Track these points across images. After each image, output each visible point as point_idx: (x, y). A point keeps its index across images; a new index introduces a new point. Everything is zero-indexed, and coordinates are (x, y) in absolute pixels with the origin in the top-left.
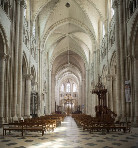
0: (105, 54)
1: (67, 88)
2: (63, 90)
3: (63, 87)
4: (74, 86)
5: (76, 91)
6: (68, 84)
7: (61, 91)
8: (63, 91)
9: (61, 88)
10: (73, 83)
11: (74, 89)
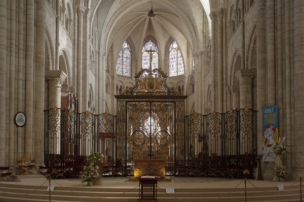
0: (251, 6)
1: (143, 61)
2: (129, 68)
3: (129, 56)
4: (173, 54)
5: (181, 73)
6: (150, 45)
7: (119, 72)
8: (128, 74)
9: (119, 61)
10: (171, 40)
11: (175, 64)
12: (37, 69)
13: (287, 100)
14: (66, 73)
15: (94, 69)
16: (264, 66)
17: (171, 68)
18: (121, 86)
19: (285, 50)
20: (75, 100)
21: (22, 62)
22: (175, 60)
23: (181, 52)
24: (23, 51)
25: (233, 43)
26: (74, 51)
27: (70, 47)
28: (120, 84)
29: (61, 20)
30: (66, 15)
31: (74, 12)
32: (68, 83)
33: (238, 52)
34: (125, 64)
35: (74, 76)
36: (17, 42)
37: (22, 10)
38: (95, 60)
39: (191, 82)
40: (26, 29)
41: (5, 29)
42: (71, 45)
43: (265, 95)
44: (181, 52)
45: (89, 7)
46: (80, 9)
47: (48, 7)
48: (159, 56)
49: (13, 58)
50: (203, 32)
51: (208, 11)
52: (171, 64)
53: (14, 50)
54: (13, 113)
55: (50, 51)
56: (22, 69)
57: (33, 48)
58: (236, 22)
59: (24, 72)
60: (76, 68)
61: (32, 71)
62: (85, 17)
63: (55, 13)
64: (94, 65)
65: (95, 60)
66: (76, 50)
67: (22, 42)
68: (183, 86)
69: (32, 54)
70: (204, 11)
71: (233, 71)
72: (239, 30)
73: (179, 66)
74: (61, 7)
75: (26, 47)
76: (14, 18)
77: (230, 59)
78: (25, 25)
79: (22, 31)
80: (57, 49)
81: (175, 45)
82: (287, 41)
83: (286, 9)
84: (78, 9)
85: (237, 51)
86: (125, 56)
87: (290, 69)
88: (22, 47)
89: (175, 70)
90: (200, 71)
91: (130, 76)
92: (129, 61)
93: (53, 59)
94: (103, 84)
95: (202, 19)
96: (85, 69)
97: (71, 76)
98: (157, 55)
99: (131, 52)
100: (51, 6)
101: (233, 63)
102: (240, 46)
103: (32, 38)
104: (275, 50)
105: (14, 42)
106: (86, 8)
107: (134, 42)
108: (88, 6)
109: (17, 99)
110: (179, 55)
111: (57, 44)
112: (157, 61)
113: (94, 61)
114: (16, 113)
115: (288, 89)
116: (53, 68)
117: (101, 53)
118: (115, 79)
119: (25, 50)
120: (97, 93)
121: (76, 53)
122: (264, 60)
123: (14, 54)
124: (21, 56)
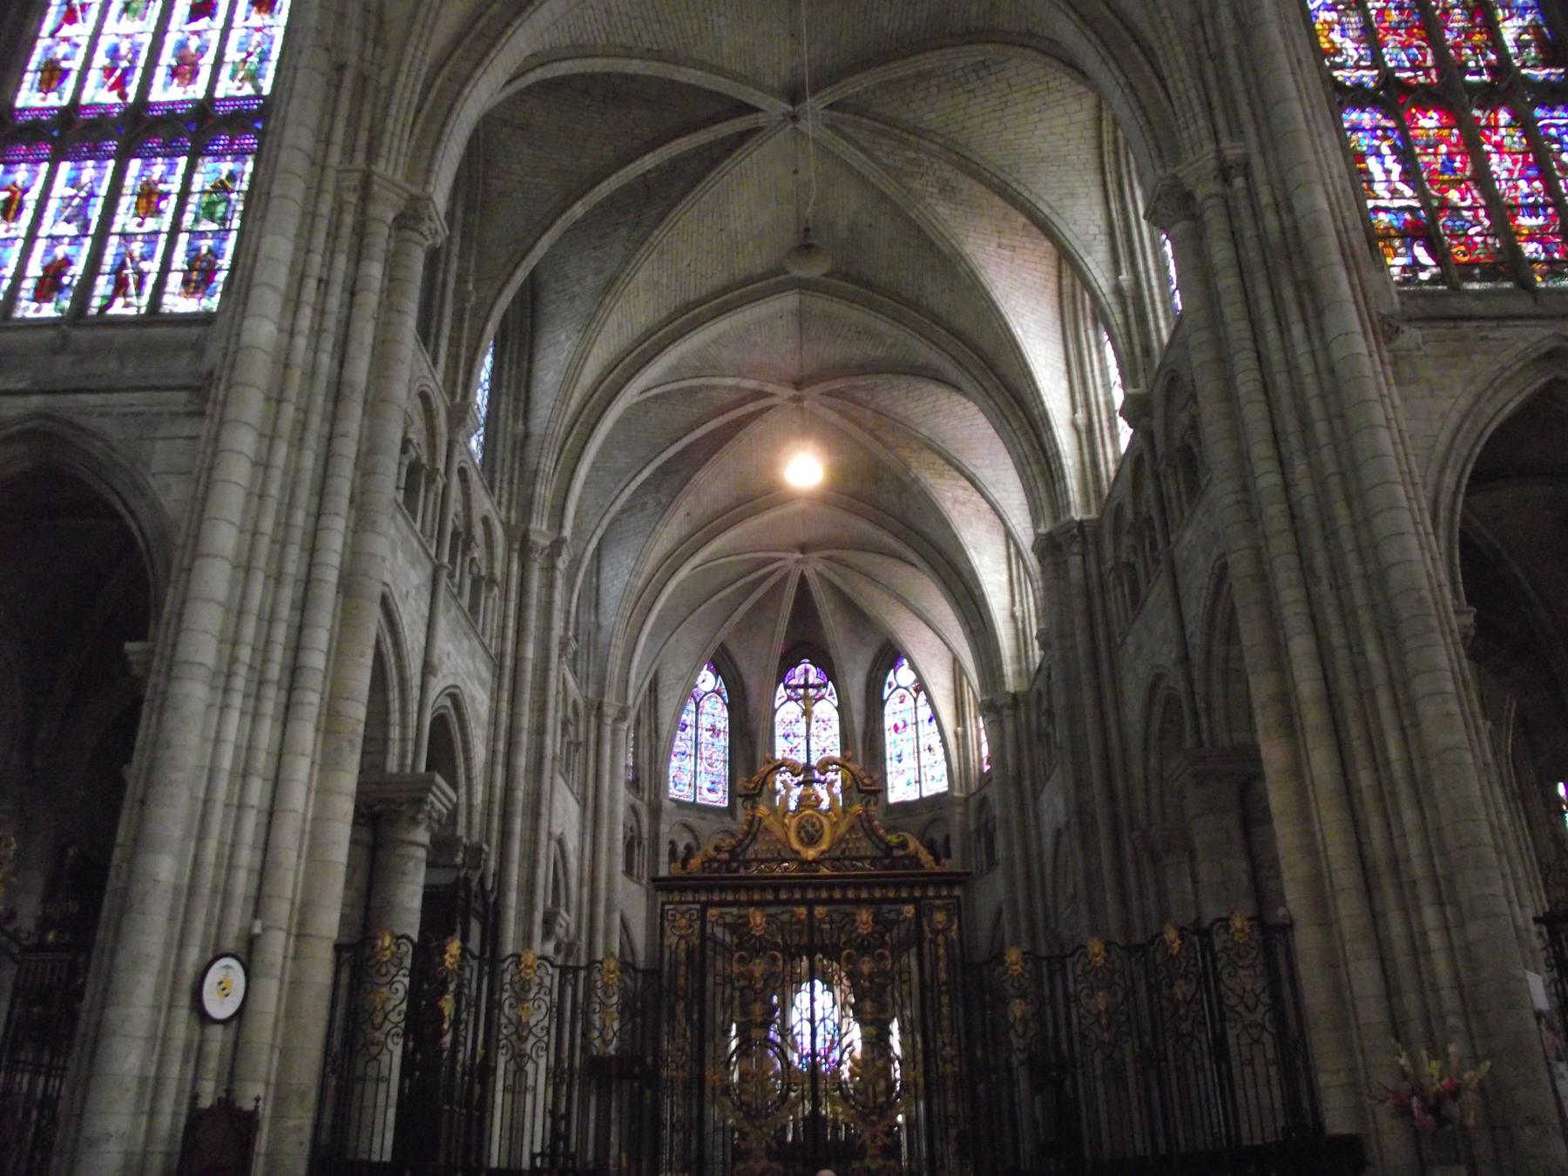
2: (722, 769)
3: (723, 724)
4: (896, 710)
8: (719, 799)
9: (682, 742)
11: (908, 749)
12: (328, 762)
13: (1418, 868)
14: (455, 788)
15: (577, 773)
16: (1290, 725)
17: (891, 766)
18: (688, 847)
19: (1363, 653)
20: (486, 904)
21: (267, 734)
22: (910, 731)
23: (930, 700)
24: (279, 689)
25: (1139, 648)
26: (495, 698)
27: (483, 684)
28: (683, 841)
29: (451, 576)
30: (473, 560)
31: (510, 550)
32: (461, 831)
33: (1163, 684)
34: (705, 754)
35: (489, 802)
36: (259, 656)
37: (297, 536)
38: (581, 738)
39: (978, 819)
40: (303, 605)
41: (219, 603)
42: (486, 674)
43: (1313, 851)
44: (930, 700)
45: (567, 532)
46: (533, 537)
47: (405, 528)
48: (842, 721)
49: (234, 717)
50: (1013, 616)
51: (1025, 532)
52: (890, 751)
53: (239, 683)
54: (193, 955)
55: (394, 694)
56: (262, 761)
57: (320, 677)
58: (1140, 566)
59: (271, 775)
60: (500, 771)
61: (302, 769)
62: (551, 568)
63: (433, 552)
64: (578, 758)
65: (581, 738)
66: (505, 695)
67: (278, 654)
68: (947, 839)
69: (312, 699)
70: (1009, 535)
71: (1153, 761)
72: (1158, 593)
73: (925, 755)
74: (455, 534)
75: (294, 670)
76: (261, 561)
77: (1134, 710)
78: (301, 586)
79: (285, 611)
80: (423, 688)
81: (903, 676)
82: (1365, 617)
83: (1337, 494)
84: (525, 539)
85: (1158, 678)
86: (705, 721)
87: (1403, 729)
88: (274, 672)
89: (913, 775)
90: (1011, 771)
91: (726, 804)
92: (723, 741)
93: (404, 727)
94: (611, 839)
95: (1004, 566)
96: (537, 768)
97: (478, 798)
98: (835, 716)
99: (730, 707)
100: (418, 527)
101: (1147, 727)
102: (1168, 655)
103: (320, 638)
104: (1323, 654)
105: (245, 654)
106: (554, 536)
107: (744, 666)
108: (561, 526)
109: (224, 893)
110: (925, 712)
111: (428, 669)
112: (838, 741)
113: (578, 745)
114: (210, 956)
115: (1409, 815)
116: (402, 765)
117: (610, 711)
118: (664, 816)
119: (285, 684)
120: (586, 874)
121: (504, 706)
122: (1285, 698)
123: (237, 701)
124: (269, 707)
